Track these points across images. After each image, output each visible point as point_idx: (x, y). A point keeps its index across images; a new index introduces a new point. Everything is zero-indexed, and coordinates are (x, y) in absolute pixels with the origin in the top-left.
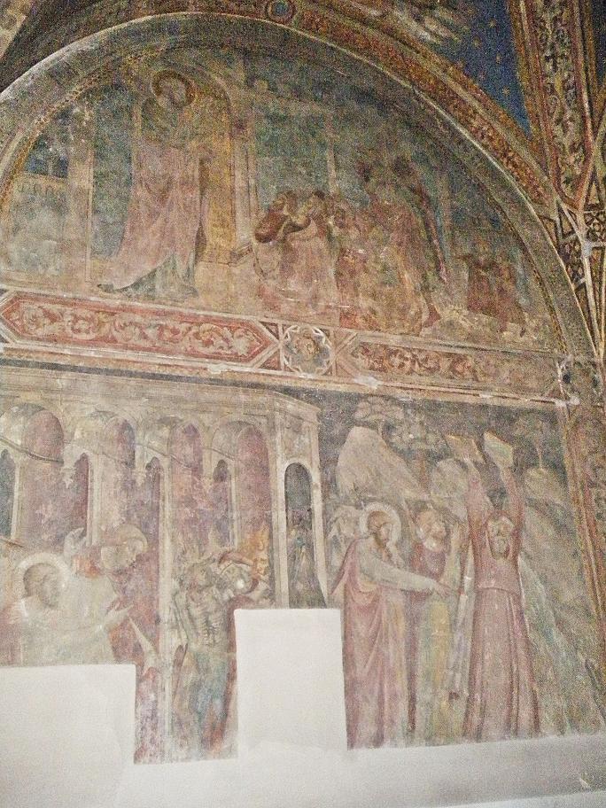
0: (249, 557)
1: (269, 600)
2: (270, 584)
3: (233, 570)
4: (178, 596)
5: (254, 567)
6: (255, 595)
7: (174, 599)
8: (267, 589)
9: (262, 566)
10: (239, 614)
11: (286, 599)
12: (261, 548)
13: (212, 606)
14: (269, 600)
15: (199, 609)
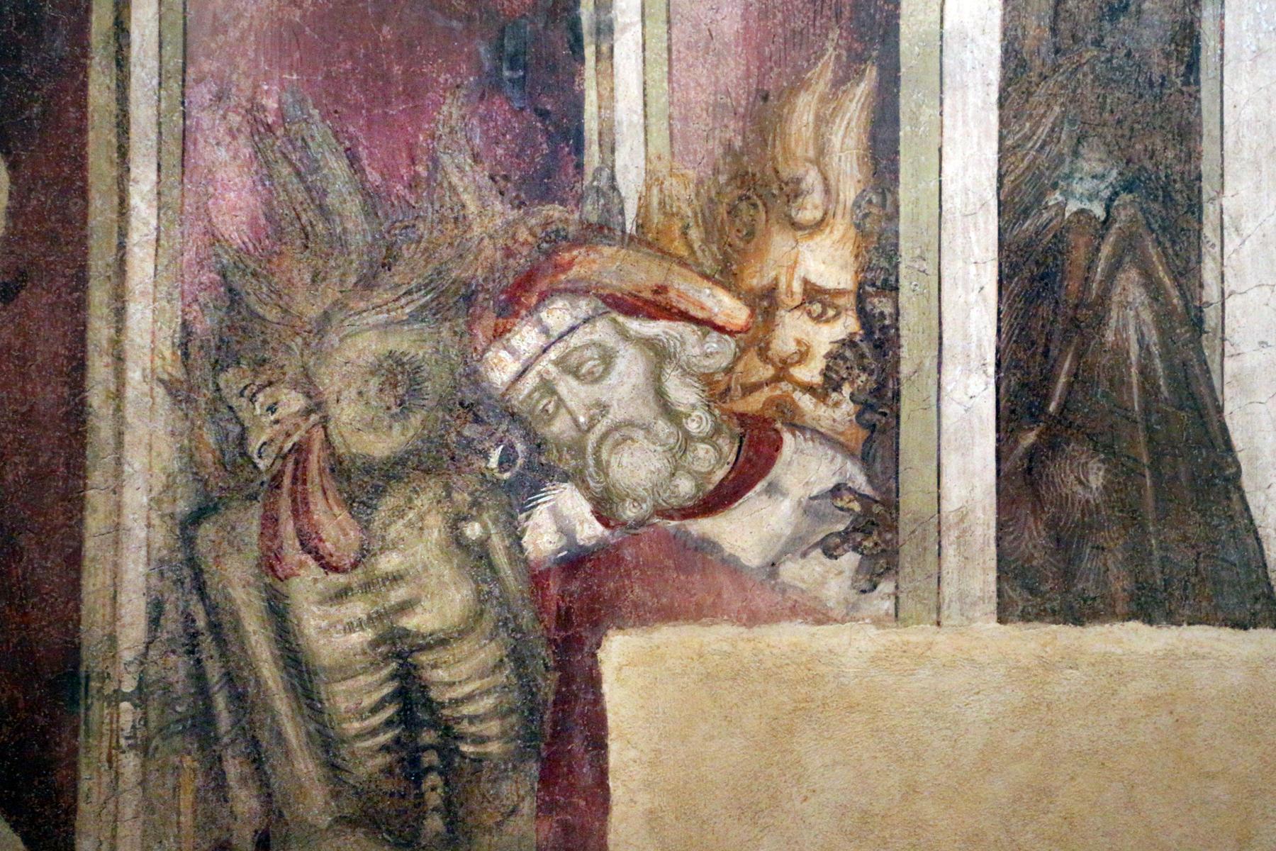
0: (727, 277)
1: (849, 560)
2: (866, 459)
3: (608, 359)
5: (755, 339)
6: (745, 531)
8: (836, 491)
11: (972, 568)
12: (809, 212)
14: (849, 560)
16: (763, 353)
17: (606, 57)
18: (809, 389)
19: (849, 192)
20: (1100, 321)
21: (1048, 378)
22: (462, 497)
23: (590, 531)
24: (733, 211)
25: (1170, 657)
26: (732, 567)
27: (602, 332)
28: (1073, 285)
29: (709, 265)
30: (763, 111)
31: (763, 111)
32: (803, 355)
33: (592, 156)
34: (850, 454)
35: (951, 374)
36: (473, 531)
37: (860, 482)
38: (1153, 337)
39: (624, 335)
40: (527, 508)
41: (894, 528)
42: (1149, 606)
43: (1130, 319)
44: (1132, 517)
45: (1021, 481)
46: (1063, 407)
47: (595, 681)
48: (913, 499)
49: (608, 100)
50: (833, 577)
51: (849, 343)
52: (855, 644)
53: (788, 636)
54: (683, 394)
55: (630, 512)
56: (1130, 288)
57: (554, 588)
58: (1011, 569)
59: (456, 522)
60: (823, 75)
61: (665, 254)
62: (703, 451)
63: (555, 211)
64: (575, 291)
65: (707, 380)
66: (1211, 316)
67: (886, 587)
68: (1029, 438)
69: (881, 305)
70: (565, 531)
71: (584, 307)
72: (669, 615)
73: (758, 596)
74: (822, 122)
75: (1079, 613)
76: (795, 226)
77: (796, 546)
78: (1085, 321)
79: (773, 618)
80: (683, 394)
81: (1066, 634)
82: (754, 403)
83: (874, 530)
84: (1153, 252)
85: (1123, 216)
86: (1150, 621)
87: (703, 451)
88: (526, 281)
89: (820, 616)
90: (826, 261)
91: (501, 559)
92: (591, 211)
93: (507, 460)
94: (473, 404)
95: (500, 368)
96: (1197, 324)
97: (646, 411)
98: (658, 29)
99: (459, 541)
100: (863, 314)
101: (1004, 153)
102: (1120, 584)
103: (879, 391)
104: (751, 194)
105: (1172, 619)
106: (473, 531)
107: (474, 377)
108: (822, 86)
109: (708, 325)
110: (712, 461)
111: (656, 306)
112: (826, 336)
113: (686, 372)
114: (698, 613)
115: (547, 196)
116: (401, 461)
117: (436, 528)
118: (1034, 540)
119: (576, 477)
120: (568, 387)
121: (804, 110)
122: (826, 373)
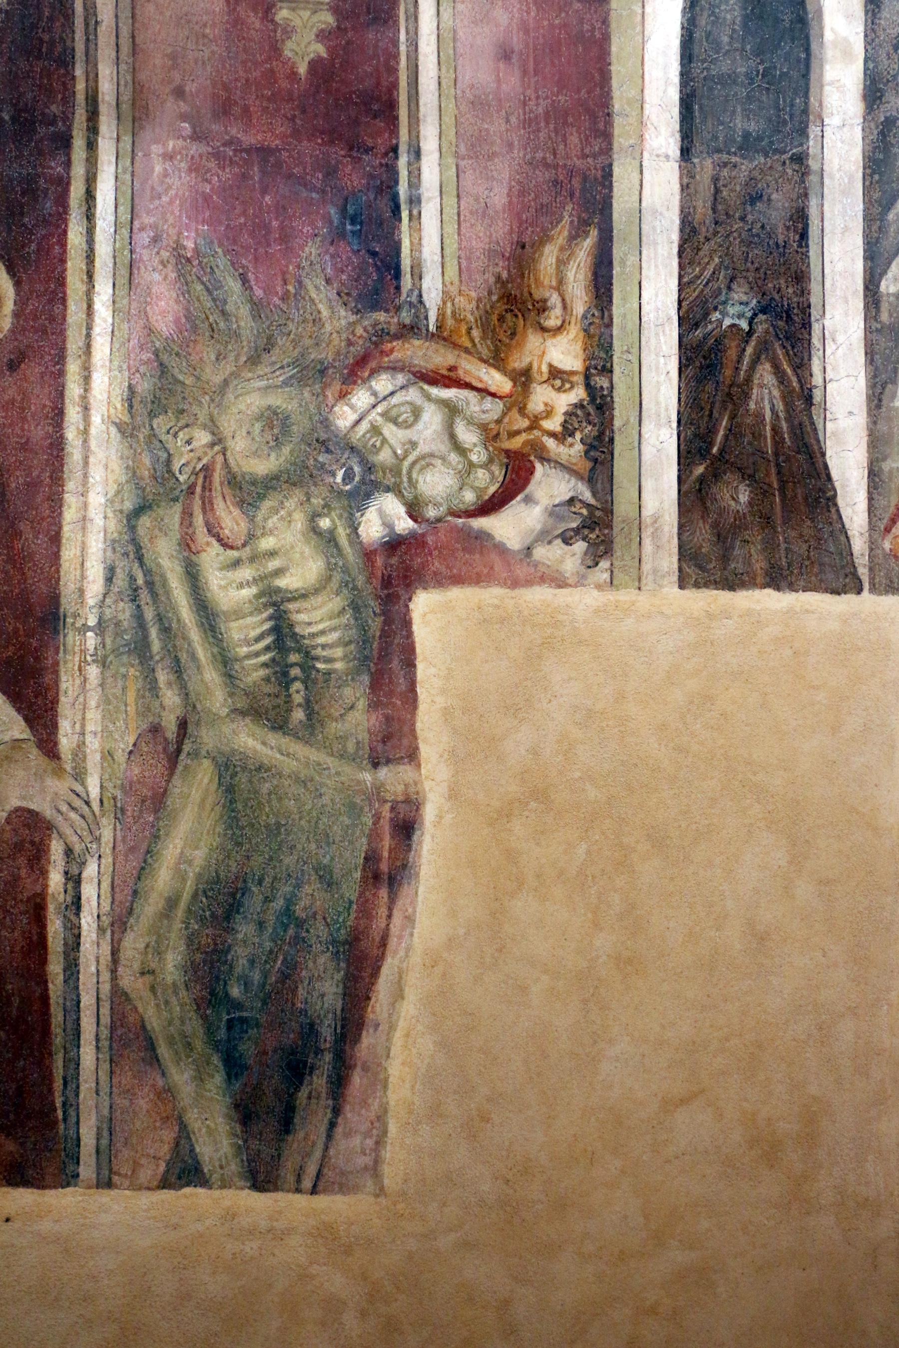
0: (497, 361)
1: (580, 546)
2: (591, 481)
3: (417, 413)
4: (145, 522)
5: (517, 402)
6: (510, 527)
7: (132, 528)
8: (571, 501)
9: (556, 402)
10: (424, 605)
11: (662, 552)
12: (552, 321)
13: (303, 570)
14: (580, 546)
15: (246, 573)
16: (522, 411)
17: (415, 218)
18: (553, 435)
19: (579, 308)
20: (747, 396)
21: (712, 431)
22: (317, 501)
23: (404, 525)
24: (501, 319)
25: (790, 612)
26: (501, 549)
27: (413, 395)
28: (728, 372)
29: (485, 353)
30: (521, 255)
31: (521, 255)
32: (549, 413)
33: (407, 282)
34: (582, 478)
35: (648, 428)
36: (325, 523)
37: (587, 496)
38: (780, 406)
39: (428, 397)
40: (362, 509)
42: (777, 579)
43: (766, 394)
44: (767, 521)
45: (694, 497)
46: (722, 451)
47: (407, 624)
48: (623, 507)
49: (417, 246)
50: (569, 557)
51: (580, 405)
52: (584, 601)
53: (538, 595)
54: (468, 436)
55: (431, 513)
56: (765, 375)
57: (379, 561)
58: (687, 554)
59: (314, 517)
60: (561, 233)
61: (456, 346)
62: (481, 473)
63: (381, 316)
64: (394, 369)
65: (484, 428)
66: (817, 395)
67: (604, 564)
68: (700, 470)
69: (601, 382)
70: (388, 525)
71: (401, 379)
72: (458, 580)
74: (561, 263)
75: (732, 583)
76: (544, 329)
77: (544, 536)
78: (737, 394)
79: (529, 583)
80: (468, 436)
81: (723, 597)
82: (516, 443)
83: (597, 527)
84: (780, 352)
85: (760, 329)
86: (778, 589)
87: (482, 476)
88: (362, 361)
89: (560, 583)
90: (564, 352)
91: (343, 541)
92: (406, 317)
93: (348, 477)
94: (325, 440)
95: (344, 417)
96: (809, 399)
97: (443, 447)
99: (315, 530)
100: (588, 386)
101: (681, 287)
102: (759, 564)
103: (600, 436)
104: (512, 307)
105: (792, 587)
106: (325, 523)
107: (326, 423)
108: (561, 240)
109: (484, 392)
110: (487, 481)
111: (449, 379)
112: (564, 401)
113: (470, 422)
114: (477, 580)
115: (375, 306)
116: (276, 477)
117: (299, 521)
118: (703, 535)
120: (389, 430)
121: (549, 256)
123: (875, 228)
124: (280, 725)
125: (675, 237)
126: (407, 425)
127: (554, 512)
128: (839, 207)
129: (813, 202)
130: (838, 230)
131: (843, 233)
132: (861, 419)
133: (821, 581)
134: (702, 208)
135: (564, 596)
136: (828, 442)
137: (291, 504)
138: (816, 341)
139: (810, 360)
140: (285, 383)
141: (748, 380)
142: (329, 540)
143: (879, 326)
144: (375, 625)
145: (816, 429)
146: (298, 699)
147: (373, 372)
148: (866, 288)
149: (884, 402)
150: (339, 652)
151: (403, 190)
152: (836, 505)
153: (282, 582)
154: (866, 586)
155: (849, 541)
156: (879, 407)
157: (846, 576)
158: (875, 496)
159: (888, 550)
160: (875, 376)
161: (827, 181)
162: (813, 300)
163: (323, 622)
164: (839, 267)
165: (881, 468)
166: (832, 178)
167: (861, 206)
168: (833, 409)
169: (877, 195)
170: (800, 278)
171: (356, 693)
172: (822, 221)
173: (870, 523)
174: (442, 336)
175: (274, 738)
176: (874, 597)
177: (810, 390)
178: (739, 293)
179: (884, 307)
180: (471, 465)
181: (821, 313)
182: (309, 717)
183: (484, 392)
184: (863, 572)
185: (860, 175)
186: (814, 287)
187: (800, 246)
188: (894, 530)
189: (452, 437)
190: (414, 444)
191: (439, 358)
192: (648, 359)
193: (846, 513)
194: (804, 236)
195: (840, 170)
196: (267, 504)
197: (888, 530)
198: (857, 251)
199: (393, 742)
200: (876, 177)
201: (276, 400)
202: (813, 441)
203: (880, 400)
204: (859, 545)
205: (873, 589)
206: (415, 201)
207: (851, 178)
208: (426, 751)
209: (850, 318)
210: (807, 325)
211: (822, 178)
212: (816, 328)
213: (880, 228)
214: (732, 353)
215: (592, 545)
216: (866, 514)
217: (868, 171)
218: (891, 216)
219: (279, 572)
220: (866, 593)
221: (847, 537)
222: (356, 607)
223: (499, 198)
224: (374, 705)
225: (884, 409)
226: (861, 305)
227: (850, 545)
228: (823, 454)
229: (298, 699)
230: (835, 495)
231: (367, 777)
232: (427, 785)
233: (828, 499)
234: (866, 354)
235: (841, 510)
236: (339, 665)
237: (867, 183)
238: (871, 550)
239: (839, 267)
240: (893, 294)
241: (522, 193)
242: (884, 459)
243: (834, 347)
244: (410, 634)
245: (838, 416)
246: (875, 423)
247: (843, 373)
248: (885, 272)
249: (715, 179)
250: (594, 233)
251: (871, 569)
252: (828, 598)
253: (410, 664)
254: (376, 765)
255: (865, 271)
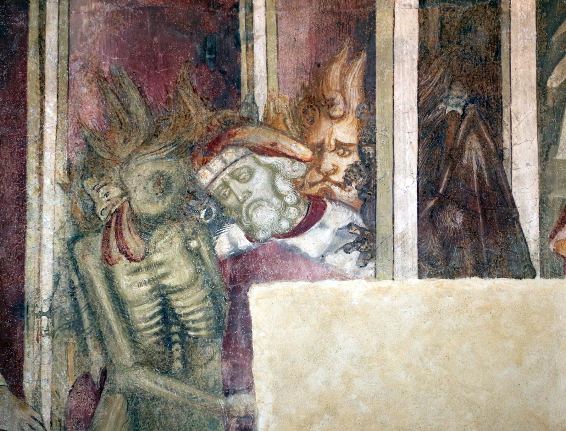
0: (303, 138)
1: (355, 254)
2: (362, 213)
3: (251, 173)
4: (79, 246)
5: (315, 163)
6: (311, 243)
7: (71, 250)
8: (350, 226)
9: (339, 164)
11: (407, 256)
13: (180, 274)
14: (355, 254)
15: (144, 276)
16: (318, 170)
17: (250, 50)
18: (338, 184)
19: (355, 104)
20: (461, 156)
21: (439, 179)
22: (188, 230)
23: (244, 244)
24: (305, 112)
26: (306, 258)
27: (249, 162)
28: (450, 141)
29: (295, 134)
30: (317, 71)
32: (335, 170)
33: (245, 90)
36: (193, 244)
37: (360, 222)
38: (483, 162)
39: (258, 163)
40: (217, 234)
41: (374, 241)
42: (481, 270)
43: (474, 155)
44: (474, 234)
45: (428, 220)
46: (445, 191)
47: (246, 305)
48: (382, 230)
49: (251, 67)
50: (348, 261)
51: (355, 165)
54: (284, 187)
55: (261, 236)
56: (474, 143)
57: (228, 267)
59: (186, 240)
61: (276, 130)
62: (292, 209)
63: (229, 112)
64: (237, 145)
65: (294, 181)
66: (506, 154)
67: (371, 265)
68: (431, 203)
69: (369, 150)
70: (234, 244)
71: (242, 151)
72: (278, 277)
73: (317, 269)
74: (343, 75)
75: (451, 275)
76: (332, 118)
77: (332, 249)
78: (455, 155)
79: (323, 278)
81: (447, 282)
82: (315, 190)
83: (366, 242)
84: (483, 128)
85: (470, 113)
86: (482, 277)
89: (343, 277)
90: (345, 132)
91: (205, 255)
92: (244, 112)
96: (501, 157)
97: (268, 194)
98: (273, 38)
99: (188, 249)
100: (360, 153)
101: (420, 88)
102: (469, 261)
103: (368, 185)
104: (313, 104)
105: (491, 275)
106: (193, 244)
107: (194, 181)
109: (294, 158)
110: (296, 215)
111: (272, 151)
112: (345, 163)
113: (285, 178)
114: (290, 277)
116: (162, 216)
117: (177, 243)
119: (239, 222)
120: (234, 185)
121: (335, 71)
122: (345, 178)
123: (544, 46)
124: (166, 371)
125: (416, 56)
126: (245, 181)
127: (338, 233)
128: (521, 34)
129: (504, 32)
130: (520, 49)
131: (523, 51)
132: (534, 168)
133: (509, 271)
134: (433, 36)
135: (345, 285)
136: (513, 183)
137: (172, 232)
138: (505, 119)
139: (502, 131)
140: (168, 156)
141: (462, 147)
142: (196, 254)
143: (546, 109)
144: (226, 307)
145: (505, 175)
146: (177, 354)
147: (223, 148)
148: (538, 85)
149: (549, 157)
150: (203, 325)
151: (242, 31)
152: (518, 222)
153: (167, 282)
154: (538, 273)
155: (527, 245)
156: (546, 159)
157: (525, 267)
158: (544, 216)
159: (552, 250)
160: (544, 141)
161: (513, 18)
162: (504, 93)
163: (192, 306)
164: (521, 71)
165: (547, 199)
166: (516, 15)
167: (535, 33)
168: (517, 162)
169: (544, 26)
170: (495, 79)
171: (214, 350)
172: (510, 43)
173: (540, 233)
174: (268, 124)
175: (161, 380)
176: (543, 280)
177: (502, 151)
178: (457, 91)
179: (550, 96)
180: (286, 205)
181: (509, 101)
182: (185, 365)
183: (294, 158)
184: (536, 264)
185: (534, 13)
186: (505, 85)
187: (496, 60)
188: (556, 237)
189: (274, 187)
190: (250, 193)
191: (265, 137)
192: (398, 134)
193: (525, 227)
194: (498, 53)
195: (521, 10)
196: (157, 233)
197: (552, 237)
198: (532, 61)
199: (238, 379)
200: (545, 14)
201: (162, 167)
202: (504, 183)
203: (547, 155)
204: (533, 247)
205: (543, 275)
206: (250, 38)
207: (528, 15)
208: (258, 384)
209: (528, 104)
210: (500, 110)
211: (510, 16)
212: (506, 111)
213: (547, 46)
214: (452, 129)
215: (364, 253)
216: (538, 228)
217: (540, 11)
218: (554, 39)
219: (164, 276)
220: (538, 277)
221: (526, 243)
222: (214, 297)
223: (303, 35)
224: (225, 357)
225: (549, 161)
226: (535, 96)
227: (528, 247)
228: (510, 191)
229: (177, 354)
230: (518, 216)
231: (221, 402)
232: (259, 406)
233: (514, 219)
234: (538, 126)
235: (522, 226)
236: (203, 333)
237: (539, 18)
238: (541, 250)
239: (521, 71)
240: (555, 88)
241: (318, 31)
242: (550, 193)
243: (517, 123)
244: (248, 312)
245: (520, 166)
246: (544, 170)
247: (523, 139)
248: (550, 74)
249: (441, 19)
250: (364, 55)
251: (541, 263)
252: (513, 281)
253: (248, 330)
254: (227, 395)
255: (537, 74)
